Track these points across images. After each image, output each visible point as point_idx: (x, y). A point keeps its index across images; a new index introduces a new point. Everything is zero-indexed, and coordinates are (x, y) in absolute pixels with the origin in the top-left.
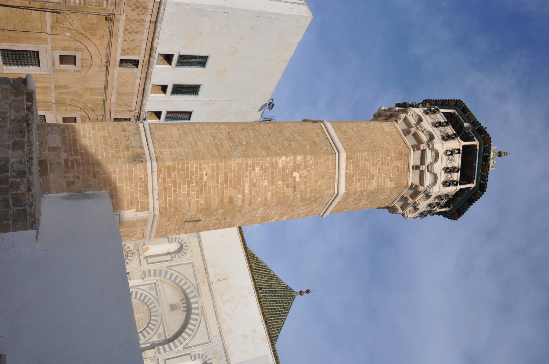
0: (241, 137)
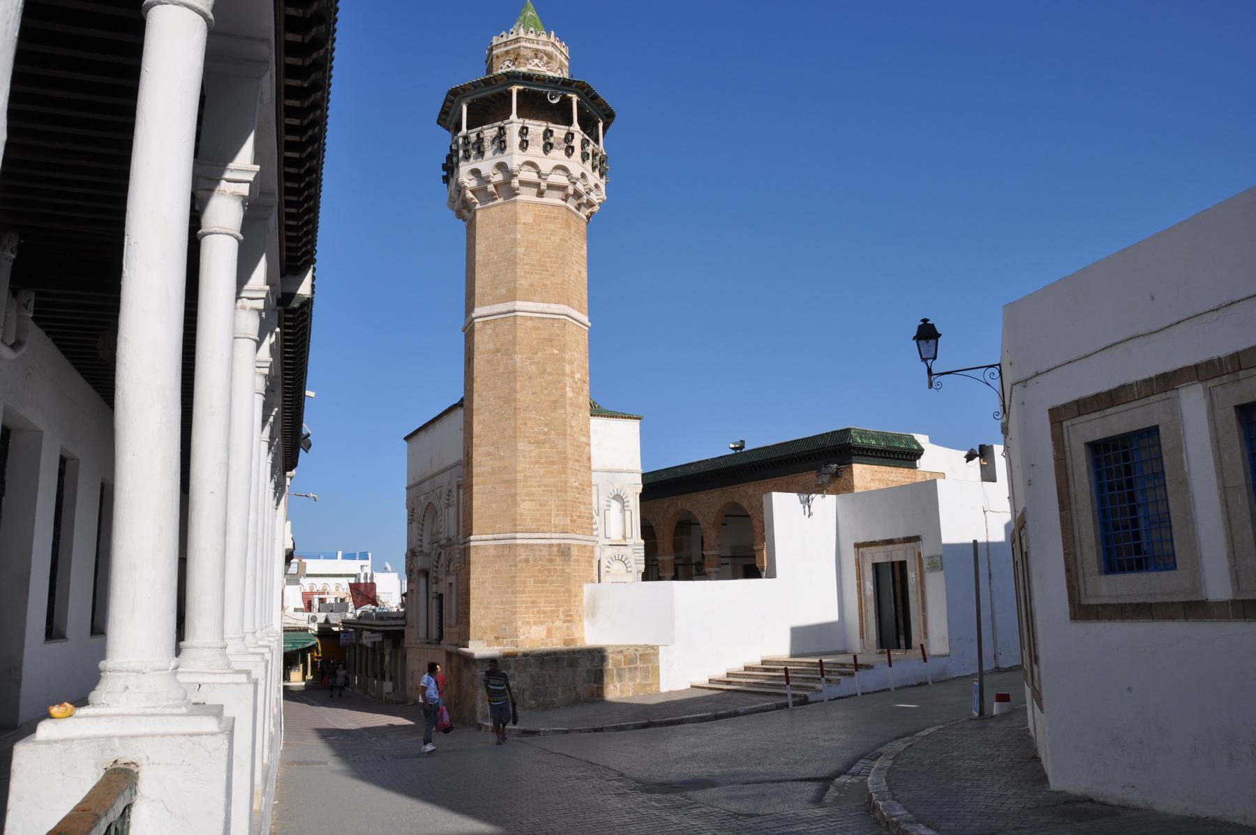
0: (537, 429)
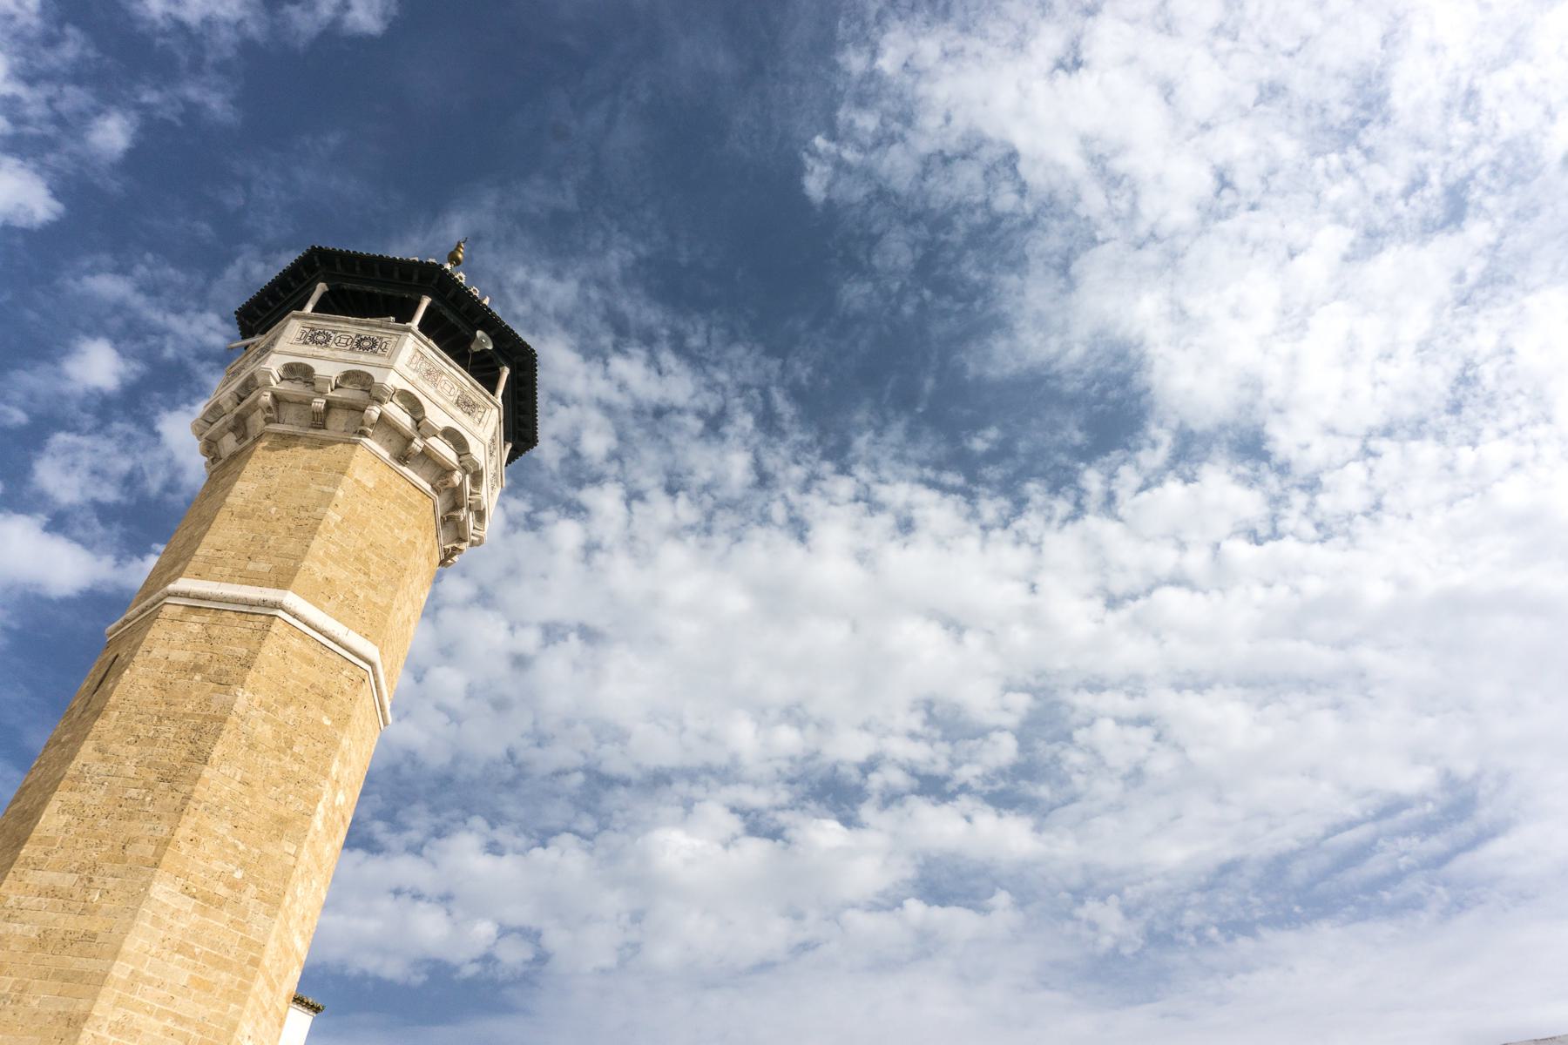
0: (217, 865)
